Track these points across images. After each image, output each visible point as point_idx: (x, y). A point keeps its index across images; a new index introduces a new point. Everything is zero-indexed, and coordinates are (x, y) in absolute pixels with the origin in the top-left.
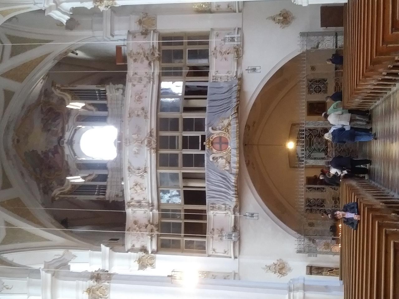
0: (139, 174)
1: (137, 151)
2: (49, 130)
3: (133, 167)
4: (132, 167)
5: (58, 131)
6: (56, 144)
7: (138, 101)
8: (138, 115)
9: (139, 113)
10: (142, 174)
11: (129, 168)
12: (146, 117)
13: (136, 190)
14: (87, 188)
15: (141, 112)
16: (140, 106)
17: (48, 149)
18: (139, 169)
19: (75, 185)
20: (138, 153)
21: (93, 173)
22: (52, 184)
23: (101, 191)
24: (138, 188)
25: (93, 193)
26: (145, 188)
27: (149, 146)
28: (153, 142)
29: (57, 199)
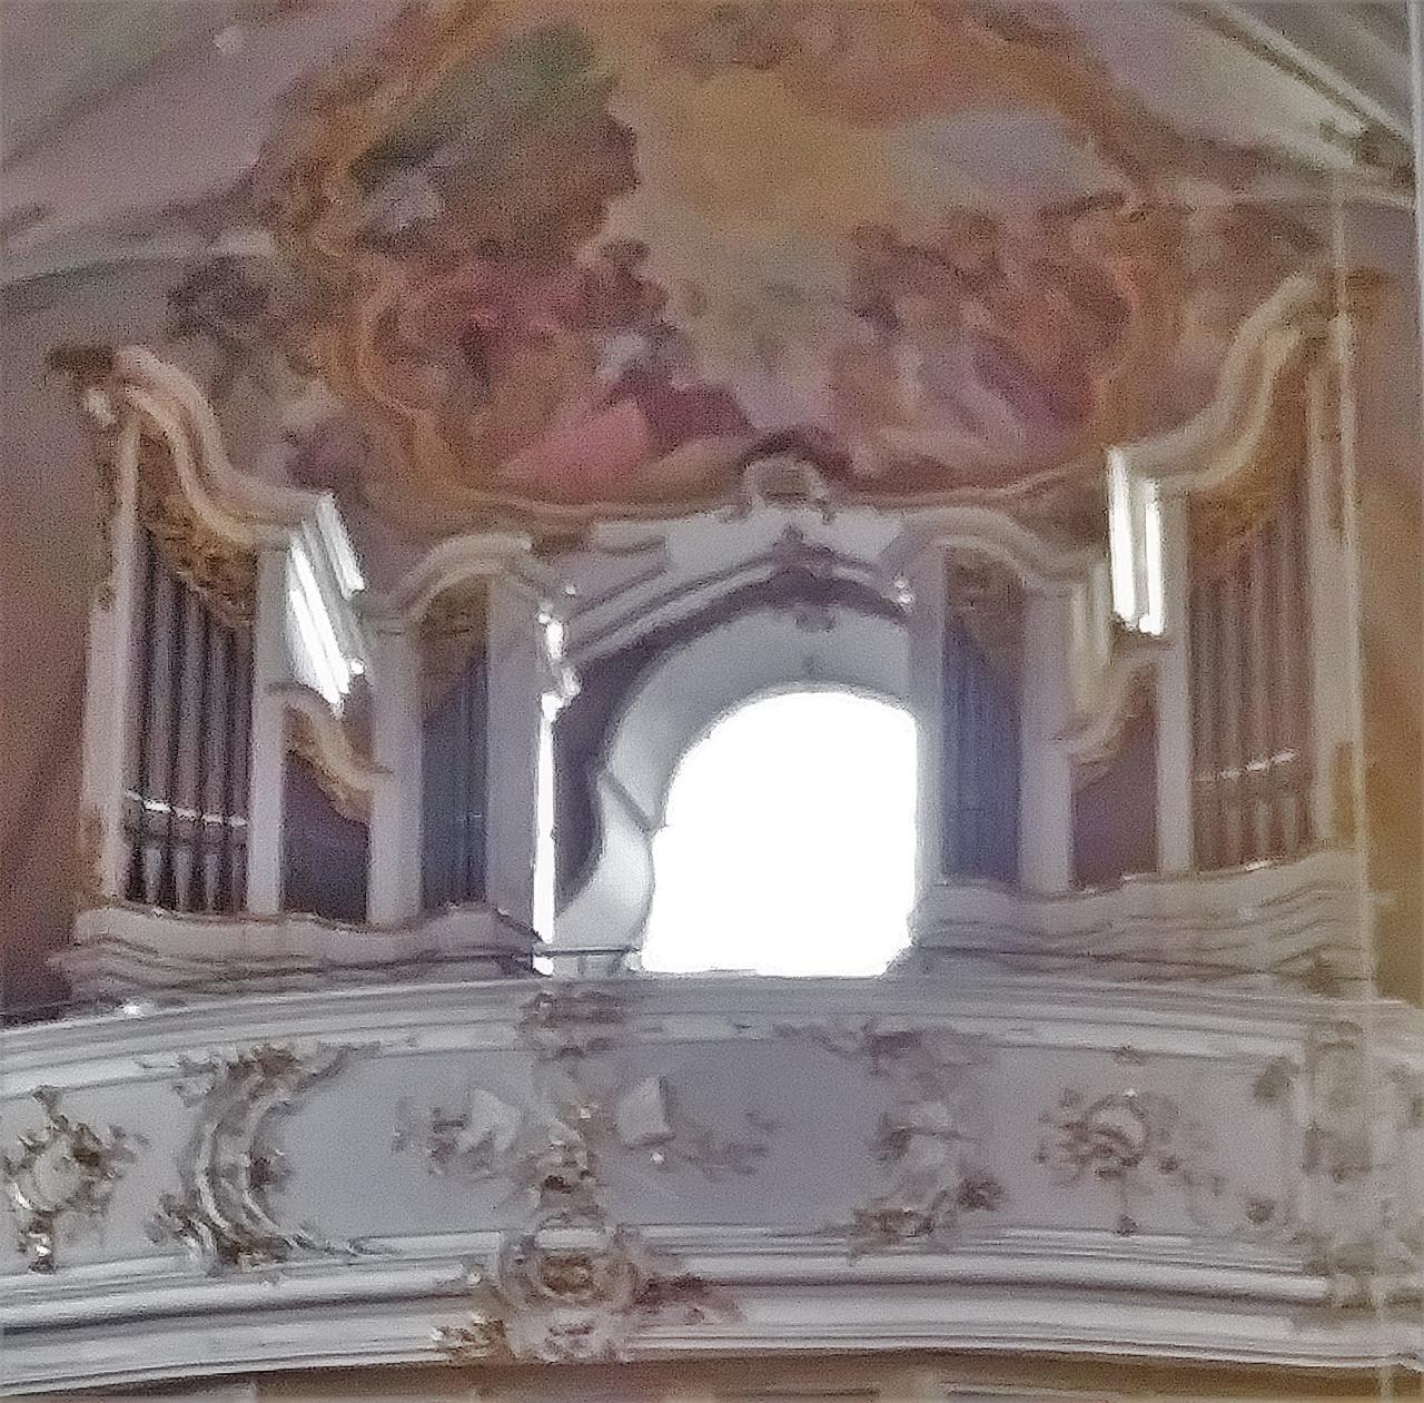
0: (202, 1182)
1: (467, 1139)
2: (879, 312)
3: (287, 1109)
4: (282, 1095)
5: (896, 418)
6: (766, 418)
7: (1079, 1130)
8: (896, 1140)
9: (927, 1155)
10: (207, 1220)
11: (275, 1064)
12: (883, 1227)
13: (26, 1165)
14: (217, 723)
15: (931, 1176)
16: (1010, 1164)
17: (672, 314)
18: (261, 1176)
19: (250, 592)
20: (443, 1152)
21: (379, 770)
22: (295, 379)
23: (183, 860)
24: (52, 1178)
25: (158, 780)
26: (46, 1265)
27: (524, 1280)
28: (576, 1317)
29: (97, 403)
